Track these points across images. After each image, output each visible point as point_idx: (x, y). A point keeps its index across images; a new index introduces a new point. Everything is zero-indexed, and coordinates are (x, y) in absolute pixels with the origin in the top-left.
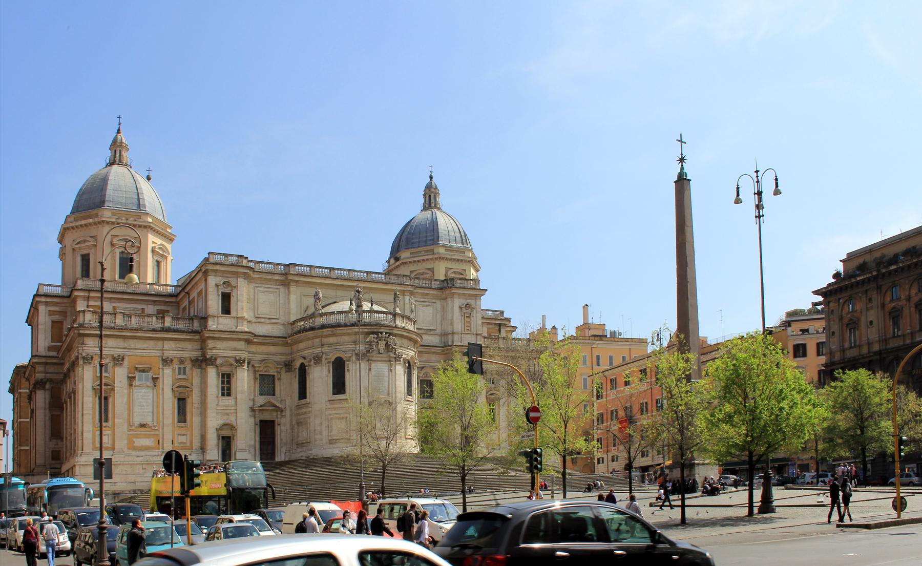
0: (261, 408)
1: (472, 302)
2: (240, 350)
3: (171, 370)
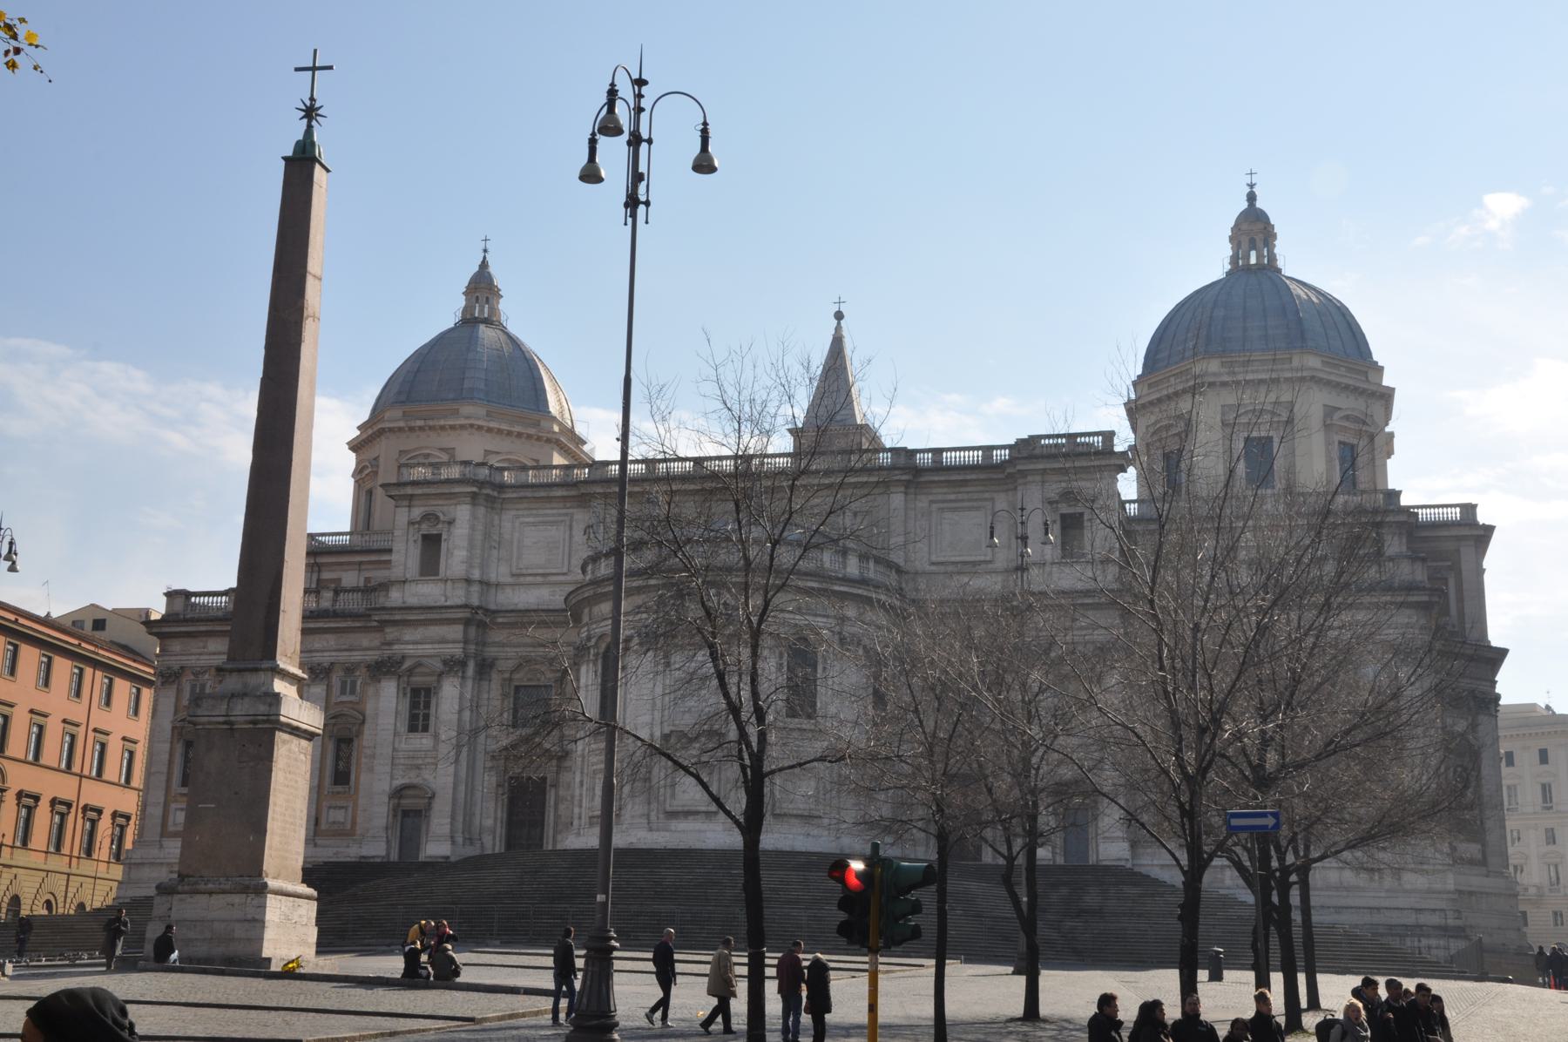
1: (1085, 485)
2: (449, 640)
3: (325, 687)
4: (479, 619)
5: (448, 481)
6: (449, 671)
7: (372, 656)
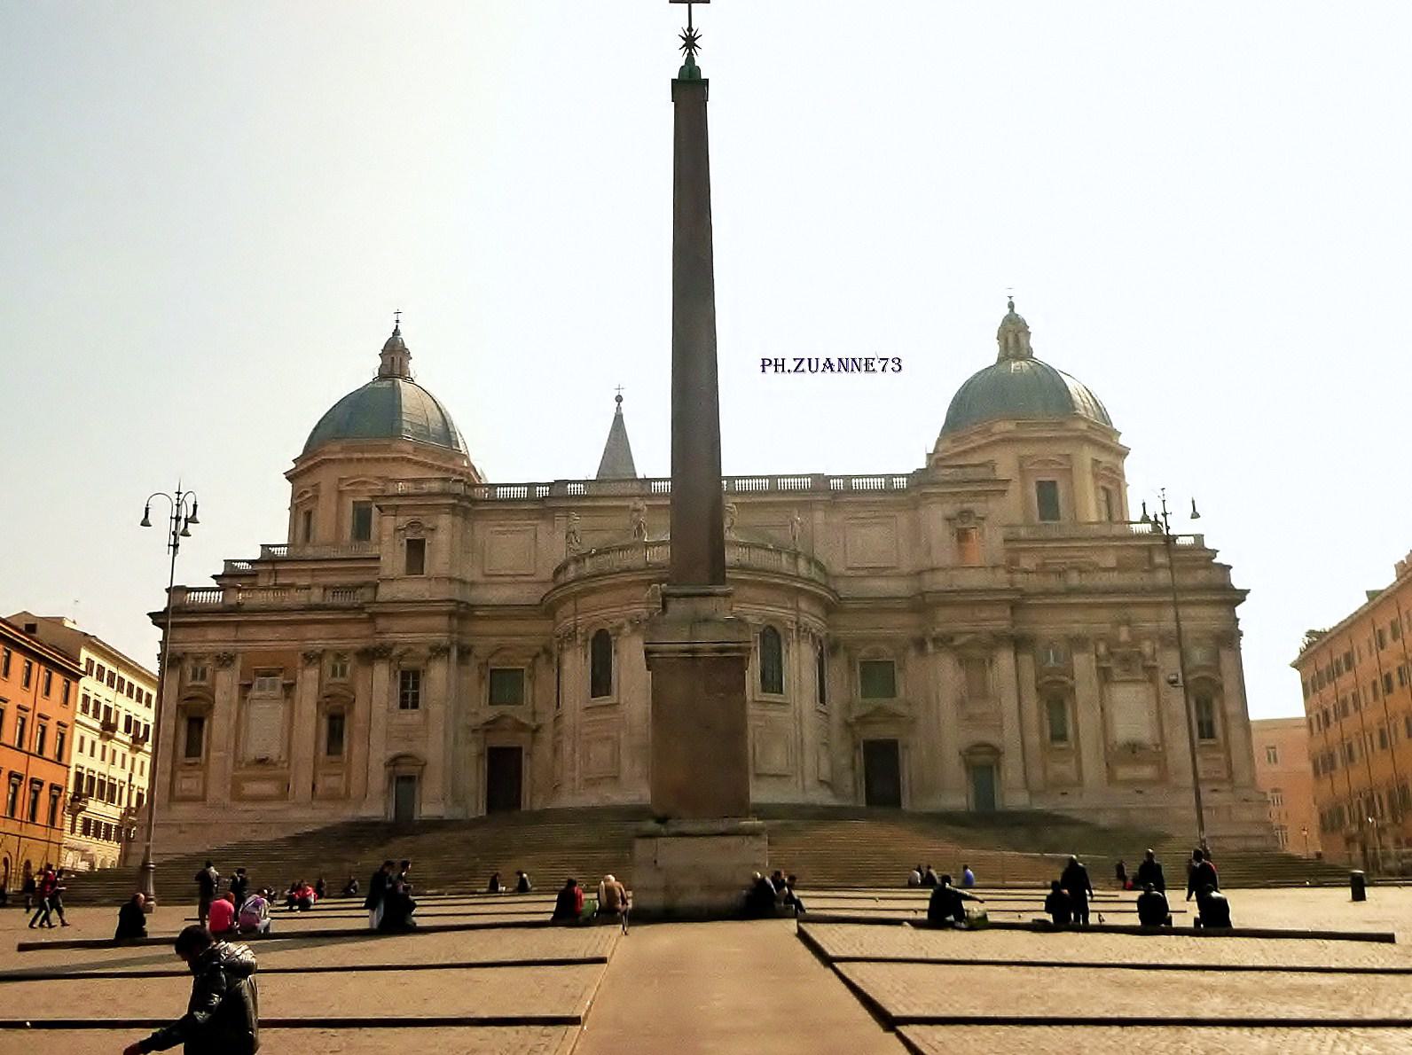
0: (488, 727)
1: (978, 507)
2: (436, 631)
4: (462, 612)
5: (430, 494)
6: (435, 658)
7: (359, 645)
